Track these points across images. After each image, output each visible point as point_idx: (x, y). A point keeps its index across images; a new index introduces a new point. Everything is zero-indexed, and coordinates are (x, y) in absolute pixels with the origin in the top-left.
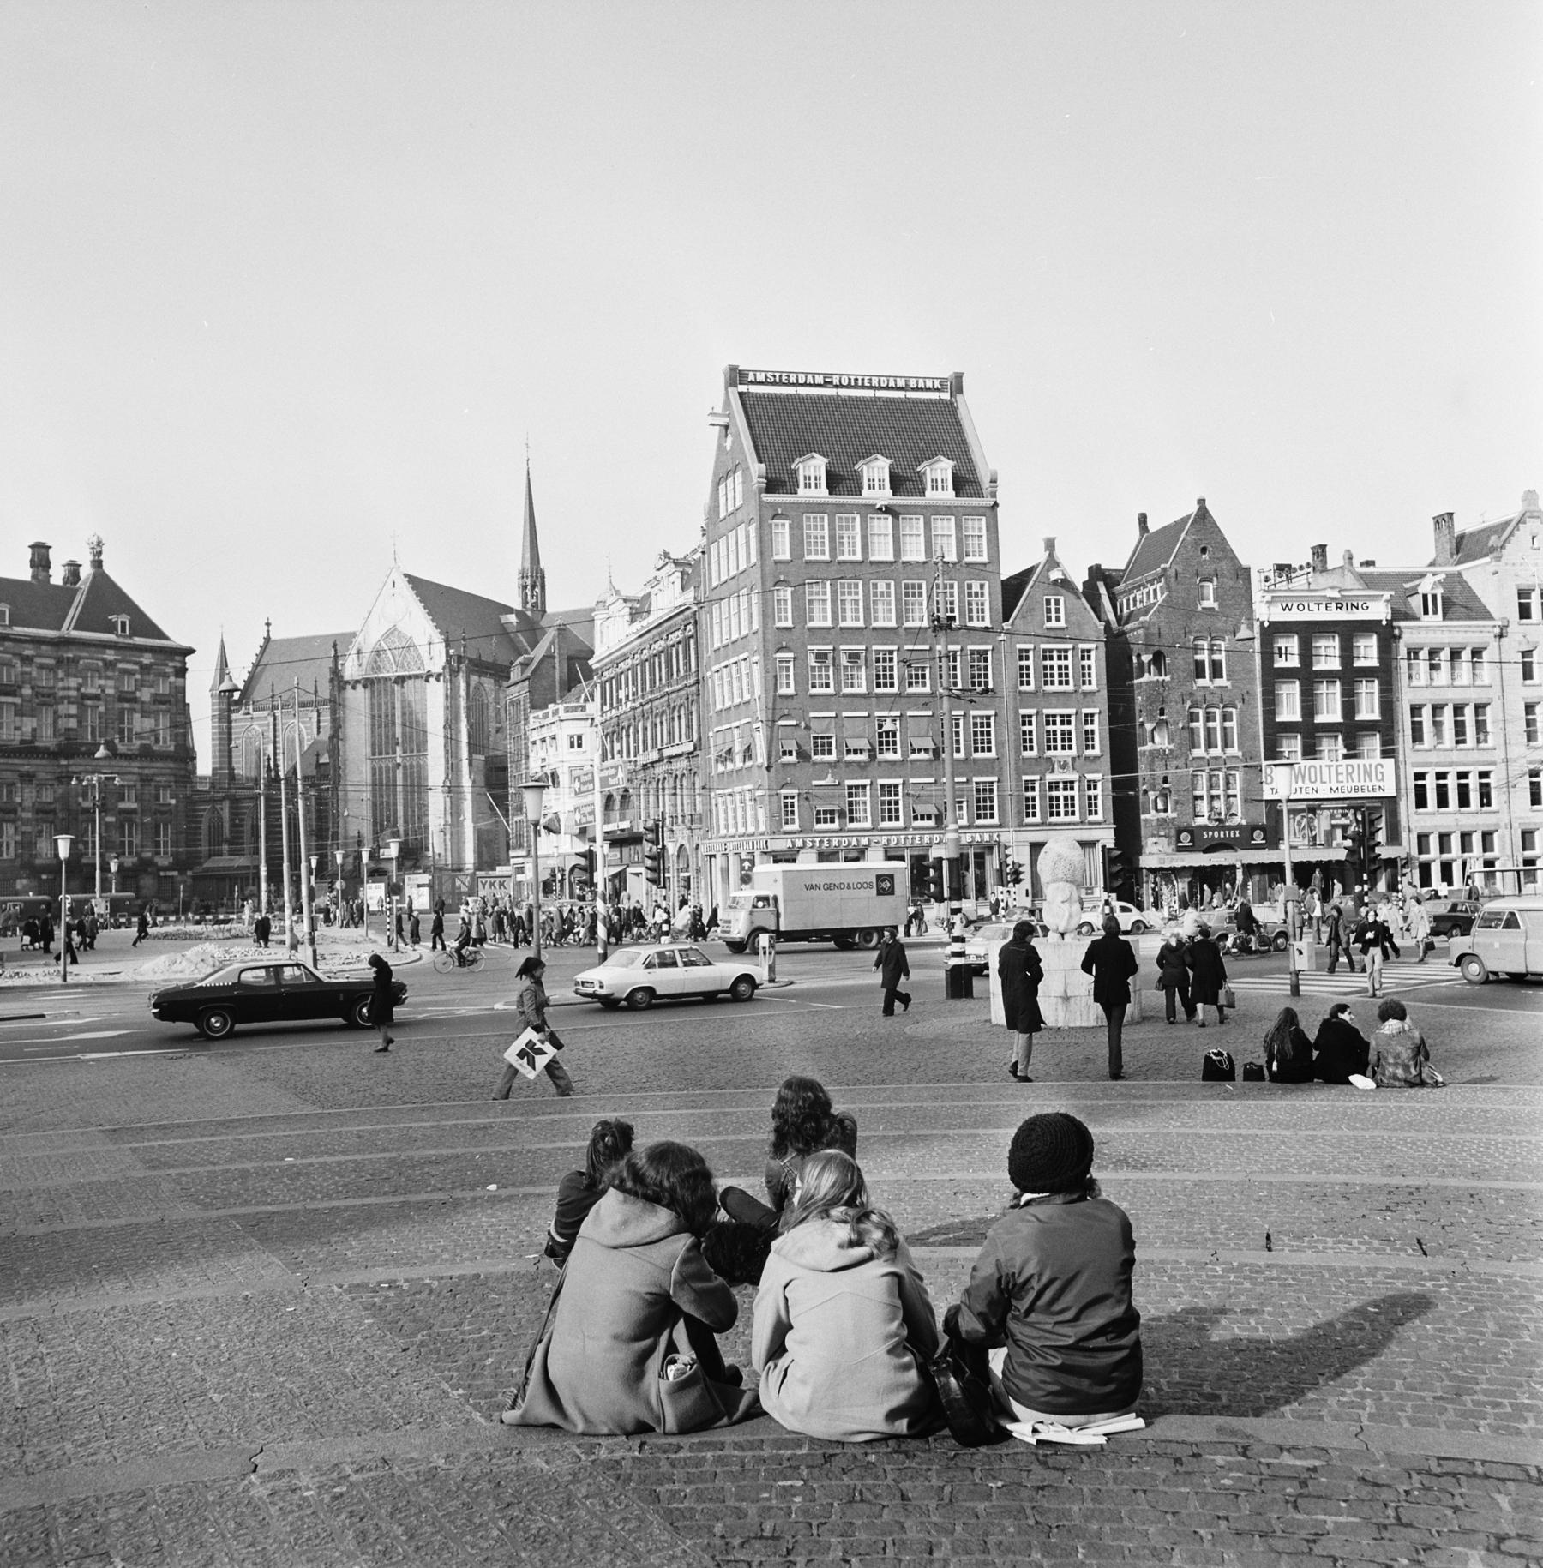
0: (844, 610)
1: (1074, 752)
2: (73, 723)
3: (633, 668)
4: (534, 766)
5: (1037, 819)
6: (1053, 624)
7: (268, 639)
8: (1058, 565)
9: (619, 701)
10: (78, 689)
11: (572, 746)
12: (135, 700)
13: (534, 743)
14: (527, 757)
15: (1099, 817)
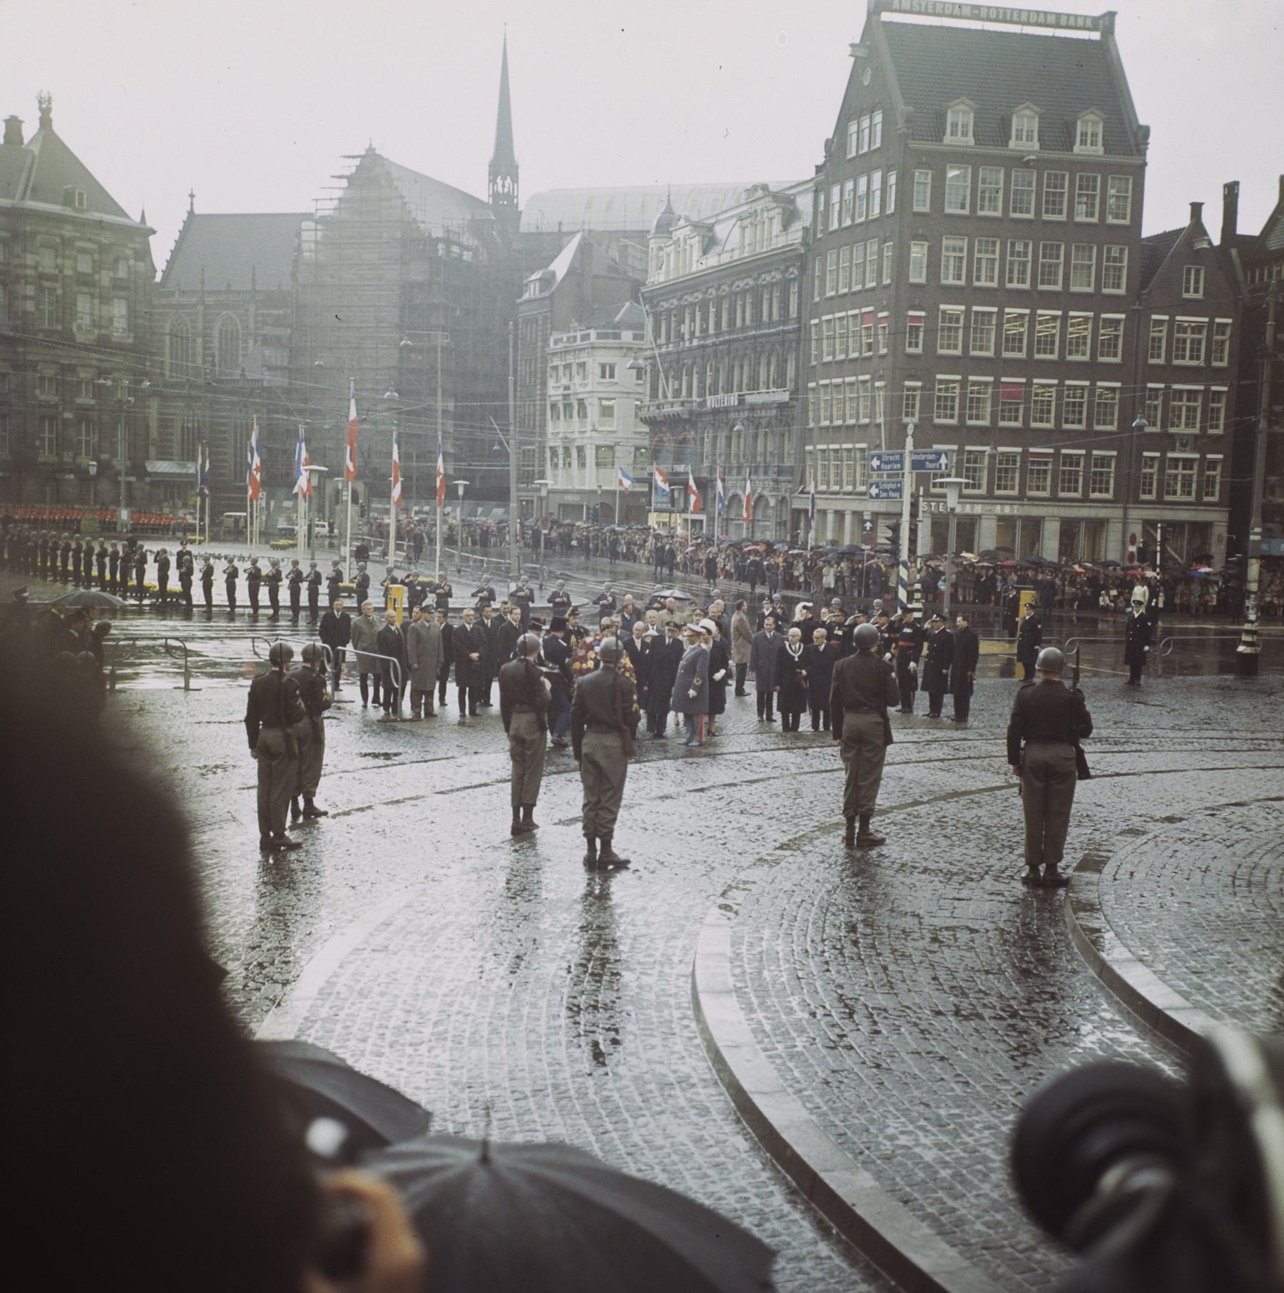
0: (979, 270)
1: (1196, 431)
2: (30, 306)
3: (704, 305)
4: (554, 391)
5: (1153, 497)
6: (1190, 295)
7: (191, 213)
8: (1205, 233)
9: (681, 337)
10: (35, 268)
11: (603, 376)
12: (92, 284)
13: (556, 368)
14: (544, 383)
15: (1215, 499)
